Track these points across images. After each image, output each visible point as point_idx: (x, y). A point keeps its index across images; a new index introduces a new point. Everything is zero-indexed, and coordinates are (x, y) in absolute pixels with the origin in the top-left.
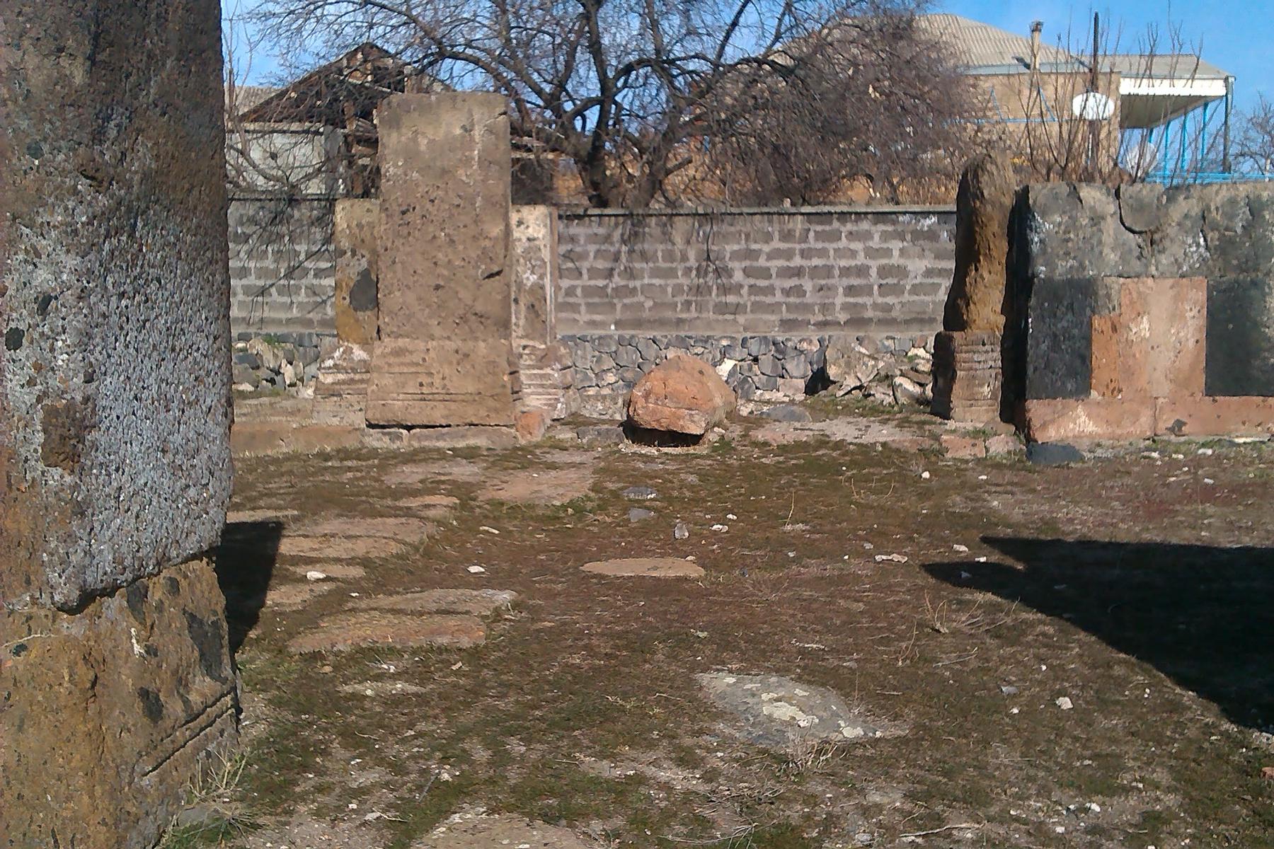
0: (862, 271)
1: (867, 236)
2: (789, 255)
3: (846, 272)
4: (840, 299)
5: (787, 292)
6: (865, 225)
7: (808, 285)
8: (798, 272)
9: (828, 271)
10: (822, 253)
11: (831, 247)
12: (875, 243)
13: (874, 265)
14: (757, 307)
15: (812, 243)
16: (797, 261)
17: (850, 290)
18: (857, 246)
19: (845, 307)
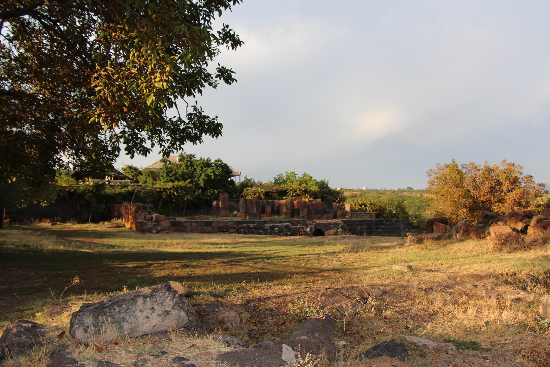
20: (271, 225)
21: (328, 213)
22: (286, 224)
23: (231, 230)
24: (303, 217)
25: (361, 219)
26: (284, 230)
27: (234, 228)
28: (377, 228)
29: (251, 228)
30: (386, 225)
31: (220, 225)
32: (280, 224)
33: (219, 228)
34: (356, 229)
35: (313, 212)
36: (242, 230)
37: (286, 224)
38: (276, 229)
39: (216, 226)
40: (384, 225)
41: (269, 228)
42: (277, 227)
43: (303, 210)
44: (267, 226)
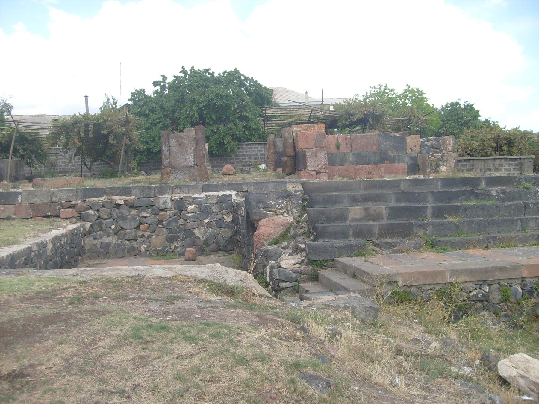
0: (257, 154)
1: (257, 148)
2: (243, 152)
3: (254, 155)
4: (253, 160)
5: (243, 159)
6: (257, 146)
7: (247, 158)
8: (245, 155)
9: (250, 155)
10: (249, 151)
11: (251, 150)
12: (259, 149)
13: (259, 153)
14: (237, 162)
15: (247, 149)
16: (244, 153)
17: (255, 158)
18: (255, 150)
19: (254, 162)
20: (177, 197)
21: (393, 161)
22: (221, 193)
23: (64, 212)
24: (318, 173)
25: (497, 174)
26: (215, 209)
27: (74, 206)
28: (439, 213)
29: (118, 206)
30: (488, 196)
31: (37, 200)
32: (203, 195)
33: (33, 207)
34: (342, 217)
35: (351, 158)
36: (91, 212)
37: (221, 193)
38: (191, 207)
39: (25, 203)
40: (477, 196)
41: (169, 204)
42: (194, 201)
43: (315, 155)
44: (165, 199)
